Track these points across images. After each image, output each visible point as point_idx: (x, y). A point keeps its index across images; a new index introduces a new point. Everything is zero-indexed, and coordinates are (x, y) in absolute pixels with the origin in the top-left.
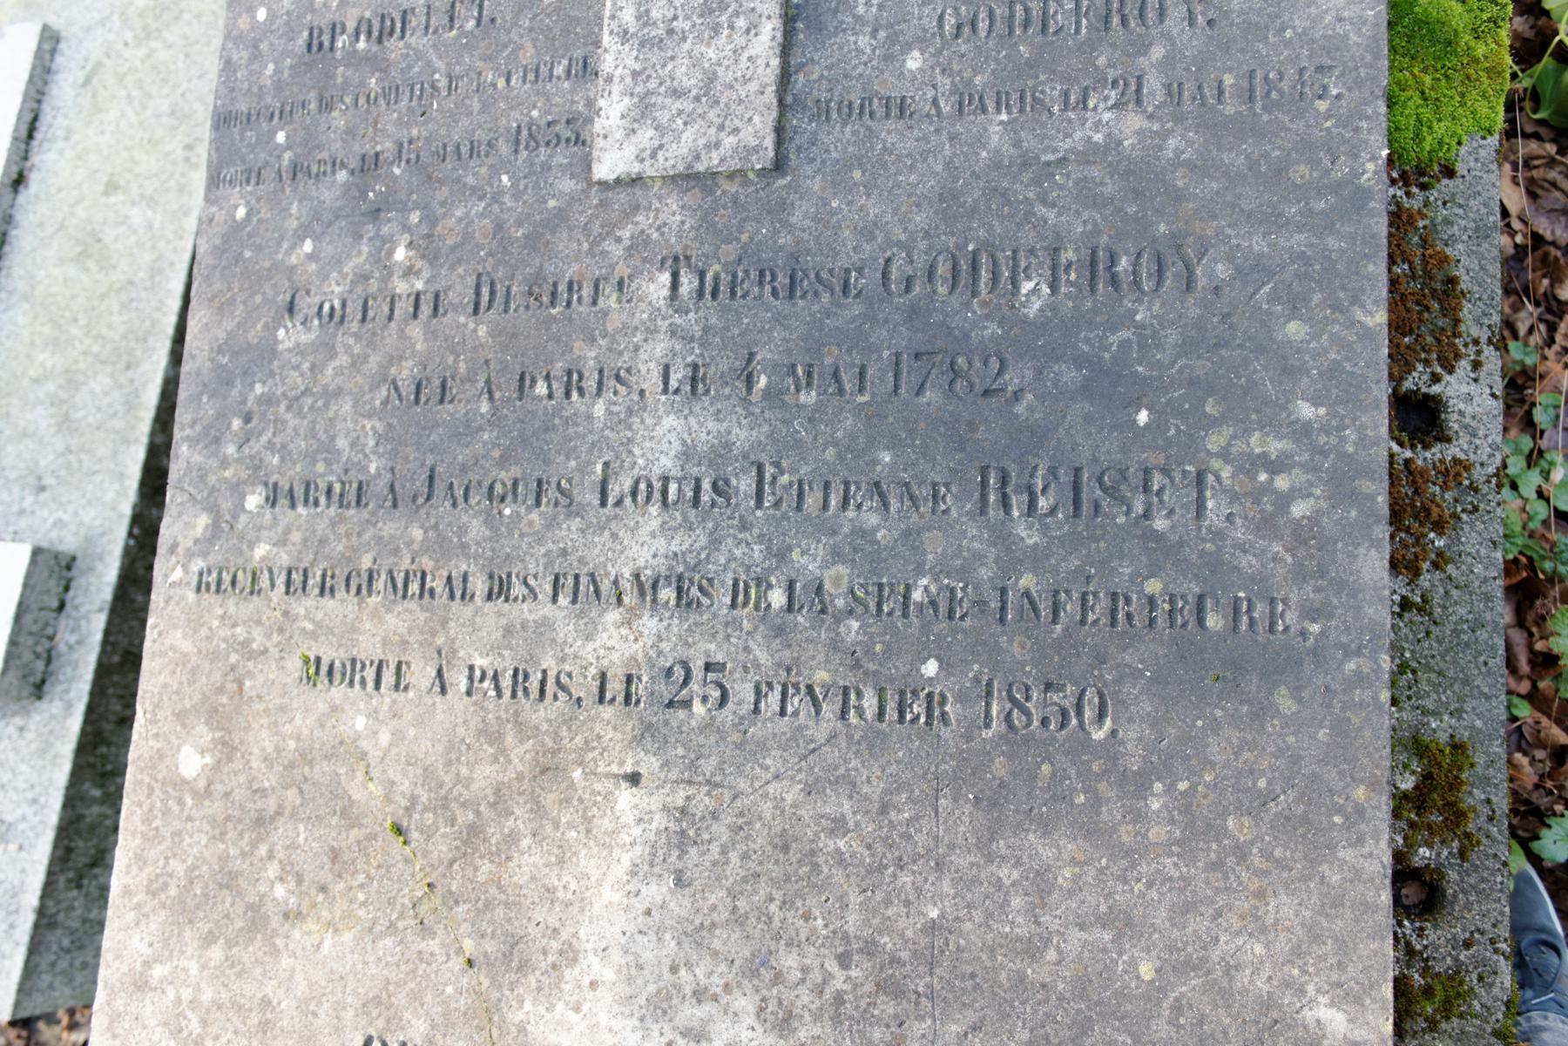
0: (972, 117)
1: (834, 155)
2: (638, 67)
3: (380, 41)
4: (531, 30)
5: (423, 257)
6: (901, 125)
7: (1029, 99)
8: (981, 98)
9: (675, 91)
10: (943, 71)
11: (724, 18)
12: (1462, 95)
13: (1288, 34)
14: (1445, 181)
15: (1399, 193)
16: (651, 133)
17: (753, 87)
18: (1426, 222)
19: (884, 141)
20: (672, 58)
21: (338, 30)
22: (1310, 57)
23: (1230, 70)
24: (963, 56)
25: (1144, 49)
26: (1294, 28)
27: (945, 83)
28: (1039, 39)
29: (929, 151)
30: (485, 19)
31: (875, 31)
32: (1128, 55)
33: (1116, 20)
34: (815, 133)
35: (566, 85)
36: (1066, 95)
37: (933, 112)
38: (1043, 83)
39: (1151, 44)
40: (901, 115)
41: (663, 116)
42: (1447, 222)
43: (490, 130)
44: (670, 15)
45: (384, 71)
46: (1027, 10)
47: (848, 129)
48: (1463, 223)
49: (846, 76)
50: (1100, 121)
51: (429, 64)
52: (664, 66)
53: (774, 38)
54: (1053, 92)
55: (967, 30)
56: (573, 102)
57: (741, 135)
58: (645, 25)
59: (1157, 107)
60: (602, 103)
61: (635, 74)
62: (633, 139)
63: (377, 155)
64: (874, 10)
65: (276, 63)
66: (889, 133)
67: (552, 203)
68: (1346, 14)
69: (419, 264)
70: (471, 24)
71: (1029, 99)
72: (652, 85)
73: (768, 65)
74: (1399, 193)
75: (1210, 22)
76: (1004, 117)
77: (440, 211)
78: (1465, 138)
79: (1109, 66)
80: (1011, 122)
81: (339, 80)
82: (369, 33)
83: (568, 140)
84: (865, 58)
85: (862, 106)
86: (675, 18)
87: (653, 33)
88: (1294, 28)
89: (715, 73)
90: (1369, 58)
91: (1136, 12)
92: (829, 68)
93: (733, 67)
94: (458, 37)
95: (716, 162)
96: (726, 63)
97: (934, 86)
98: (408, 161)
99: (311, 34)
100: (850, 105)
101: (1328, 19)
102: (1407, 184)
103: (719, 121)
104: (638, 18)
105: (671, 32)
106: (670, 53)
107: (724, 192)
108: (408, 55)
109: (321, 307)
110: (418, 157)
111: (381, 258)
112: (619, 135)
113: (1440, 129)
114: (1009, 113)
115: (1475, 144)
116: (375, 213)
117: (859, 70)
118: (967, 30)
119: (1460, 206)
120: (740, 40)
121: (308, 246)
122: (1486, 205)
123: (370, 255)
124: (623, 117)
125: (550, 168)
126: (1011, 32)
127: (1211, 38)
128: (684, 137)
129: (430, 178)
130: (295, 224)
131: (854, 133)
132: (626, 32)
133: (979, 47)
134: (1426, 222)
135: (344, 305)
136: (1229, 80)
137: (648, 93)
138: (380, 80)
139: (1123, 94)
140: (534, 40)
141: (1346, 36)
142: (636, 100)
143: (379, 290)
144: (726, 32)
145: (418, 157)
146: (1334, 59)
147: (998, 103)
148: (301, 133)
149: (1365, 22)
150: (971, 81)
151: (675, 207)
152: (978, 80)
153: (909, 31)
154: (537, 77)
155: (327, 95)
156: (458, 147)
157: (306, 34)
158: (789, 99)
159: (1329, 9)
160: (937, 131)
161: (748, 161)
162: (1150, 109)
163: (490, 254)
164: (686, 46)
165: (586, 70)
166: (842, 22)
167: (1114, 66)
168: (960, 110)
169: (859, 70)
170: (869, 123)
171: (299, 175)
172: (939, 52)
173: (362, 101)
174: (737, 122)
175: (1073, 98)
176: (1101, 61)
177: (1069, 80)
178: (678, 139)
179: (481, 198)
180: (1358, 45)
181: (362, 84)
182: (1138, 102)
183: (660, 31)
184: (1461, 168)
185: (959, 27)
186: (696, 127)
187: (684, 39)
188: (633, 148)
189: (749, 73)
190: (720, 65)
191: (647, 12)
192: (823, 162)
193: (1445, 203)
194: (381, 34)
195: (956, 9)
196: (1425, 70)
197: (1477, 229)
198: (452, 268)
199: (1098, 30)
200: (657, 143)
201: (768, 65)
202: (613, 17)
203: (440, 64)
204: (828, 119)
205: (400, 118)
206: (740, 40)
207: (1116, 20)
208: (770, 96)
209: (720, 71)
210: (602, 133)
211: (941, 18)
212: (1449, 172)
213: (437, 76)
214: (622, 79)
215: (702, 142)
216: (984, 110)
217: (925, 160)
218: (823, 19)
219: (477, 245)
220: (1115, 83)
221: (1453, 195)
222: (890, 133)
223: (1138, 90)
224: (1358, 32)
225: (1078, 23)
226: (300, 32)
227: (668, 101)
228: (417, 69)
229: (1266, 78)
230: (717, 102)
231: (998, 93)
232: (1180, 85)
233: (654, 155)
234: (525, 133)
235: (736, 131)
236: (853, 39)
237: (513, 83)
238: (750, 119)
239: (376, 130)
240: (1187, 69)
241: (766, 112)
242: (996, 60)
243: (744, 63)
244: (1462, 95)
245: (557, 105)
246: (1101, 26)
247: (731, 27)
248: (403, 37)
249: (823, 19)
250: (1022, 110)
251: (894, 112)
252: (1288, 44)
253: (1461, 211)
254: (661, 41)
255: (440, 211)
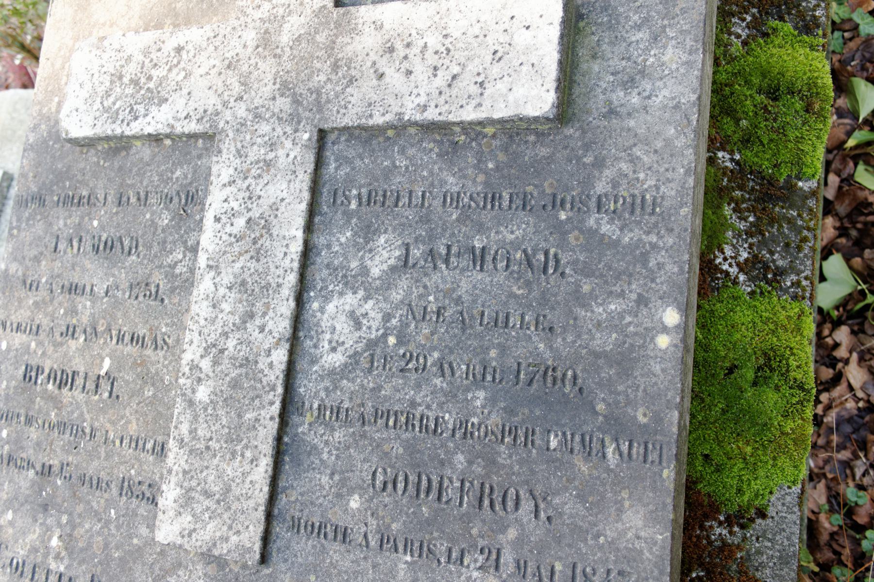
0: (388, 554)
1: (300, 560)
2: (187, 468)
3: (60, 387)
4: (137, 412)
5: (66, 549)
6: (343, 548)
7: (425, 549)
8: (395, 540)
9: (206, 492)
10: (372, 515)
11: (239, 448)
12: (774, 459)
13: (602, 540)
14: (759, 521)
15: (724, 532)
16: (189, 518)
17: (251, 503)
18: (743, 553)
19: (332, 558)
20: (207, 467)
21: (40, 372)
22: (615, 562)
23: (560, 559)
24: (386, 506)
25: (504, 529)
26: (606, 536)
27: (373, 523)
28: (436, 505)
29: (358, 572)
30: (114, 395)
31: (332, 474)
32: (493, 531)
33: (486, 502)
34: (289, 541)
35: (151, 458)
36: (450, 551)
37: (364, 543)
38: (434, 539)
39: (508, 526)
40: (344, 541)
41: (198, 509)
42: (759, 552)
43: (108, 474)
44: (208, 436)
45: (59, 409)
46: (429, 481)
47: (310, 543)
48: (771, 553)
49: (312, 503)
50: (471, 576)
51: (82, 414)
52: (201, 472)
53: (266, 471)
54: (441, 547)
55: (390, 486)
56: (153, 472)
57: (241, 537)
58: (194, 438)
59: (509, 575)
60: (164, 487)
61: (185, 472)
62: (179, 519)
63: (50, 466)
64: (333, 458)
65: (8, 382)
66: (335, 552)
67: (135, 541)
68: (643, 534)
69: (63, 553)
70: (106, 395)
71: (425, 549)
72: (194, 483)
73: (261, 490)
74: (724, 532)
75: (549, 519)
76: (408, 558)
77: (78, 521)
78: (775, 490)
79: (479, 536)
80: (413, 563)
81: (37, 407)
82: (55, 379)
83: (148, 499)
84: (324, 493)
85: (320, 527)
86: (211, 439)
87: (198, 446)
88: (606, 536)
89: (230, 486)
90: (656, 573)
91: (500, 499)
92: (302, 494)
93: (241, 485)
94: (99, 401)
95: (225, 551)
96: (238, 481)
97: (366, 524)
98: (65, 478)
99: (26, 368)
100: (313, 526)
101: (630, 535)
102: (730, 525)
103: (229, 522)
104: (190, 432)
105: (208, 448)
106: (206, 464)
107: (231, 570)
108: (72, 403)
109: (12, 560)
110: (70, 477)
111: (45, 540)
112: (172, 513)
113: (755, 485)
114: (412, 556)
115: (783, 493)
116: (45, 508)
117: (320, 501)
118: (390, 486)
119: (769, 540)
120: (247, 468)
121: (10, 515)
122: (788, 539)
123: (40, 536)
124: (175, 501)
125: (137, 515)
126: (418, 495)
127: (549, 531)
128: (209, 527)
129: (75, 495)
130: (5, 497)
131: (314, 547)
132: (182, 440)
133: (397, 502)
134: (743, 553)
135: (24, 564)
136: (558, 567)
137: (191, 489)
138: (56, 415)
139: (487, 559)
140: (138, 419)
141: (641, 552)
142: (183, 491)
143: (42, 562)
144: (239, 458)
145: (70, 477)
146: (632, 568)
147: (406, 546)
148: (14, 435)
149: (655, 543)
150: (389, 526)
151: (200, 574)
152: (394, 526)
153: (354, 479)
154: (137, 446)
155: (30, 414)
156: (91, 479)
157: (24, 367)
158: (276, 511)
159: (631, 527)
160: (365, 558)
161: (244, 557)
162: (504, 576)
163: (100, 563)
164: (216, 461)
165: (161, 451)
166: (313, 463)
167: (483, 537)
168: (381, 546)
169: (320, 501)
170: (323, 541)
171: (11, 464)
172: (371, 499)
173: (47, 426)
174: (239, 526)
175: (454, 555)
176: (475, 531)
177: (451, 540)
178: (204, 528)
179: (99, 520)
180: (650, 560)
181: (48, 414)
182: (497, 568)
183: (201, 446)
184: (771, 511)
185: (385, 484)
186: (216, 522)
187: (215, 456)
188: (178, 525)
189: (250, 492)
190: (234, 481)
191: (196, 429)
192: (293, 563)
193: (757, 539)
194: (61, 383)
195: (384, 469)
196: (748, 443)
197: (780, 558)
198: (80, 564)
199: (474, 506)
200: (192, 527)
201: (261, 490)
202: (176, 427)
203: (87, 416)
204: (298, 531)
205: (64, 446)
206: (247, 468)
207: (486, 502)
208: (260, 514)
209: (233, 485)
210: (162, 509)
211: (374, 474)
212: (762, 514)
213: (85, 424)
214: (177, 474)
215: (218, 534)
216: (396, 551)
217: (357, 578)
218: (301, 457)
219: (94, 553)
220: (482, 551)
221: (765, 531)
222: (335, 551)
223: (498, 559)
224: (650, 550)
225: (461, 498)
226: (21, 365)
227: (201, 498)
228: (75, 415)
229: (584, 571)
230: (229, 508)
231: (406, 539)
232: (525, 562)
233: (190, 535)
234: (126, 484)
235: (238, 532)
236: (318, 476)
237: (124, 445)
238: (247, 527)
239: (51, 449)
240: (531, 551)
241: (257, 525)
242: (407, 514)
243: (247, 485)
244: (774, 459)
245: (145, 471)
246: (476, 504)
247: (243, 455)
248: (71, 389)
249: (301, 457)
250: (420, 556)
251: (340, 537)
252: (601, 547)
253: (770, 544)
254: (202, 453)
255: (78, 521)
